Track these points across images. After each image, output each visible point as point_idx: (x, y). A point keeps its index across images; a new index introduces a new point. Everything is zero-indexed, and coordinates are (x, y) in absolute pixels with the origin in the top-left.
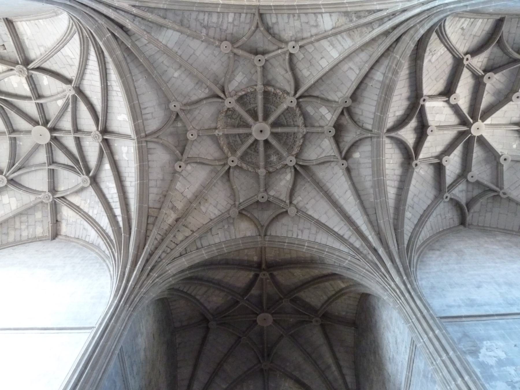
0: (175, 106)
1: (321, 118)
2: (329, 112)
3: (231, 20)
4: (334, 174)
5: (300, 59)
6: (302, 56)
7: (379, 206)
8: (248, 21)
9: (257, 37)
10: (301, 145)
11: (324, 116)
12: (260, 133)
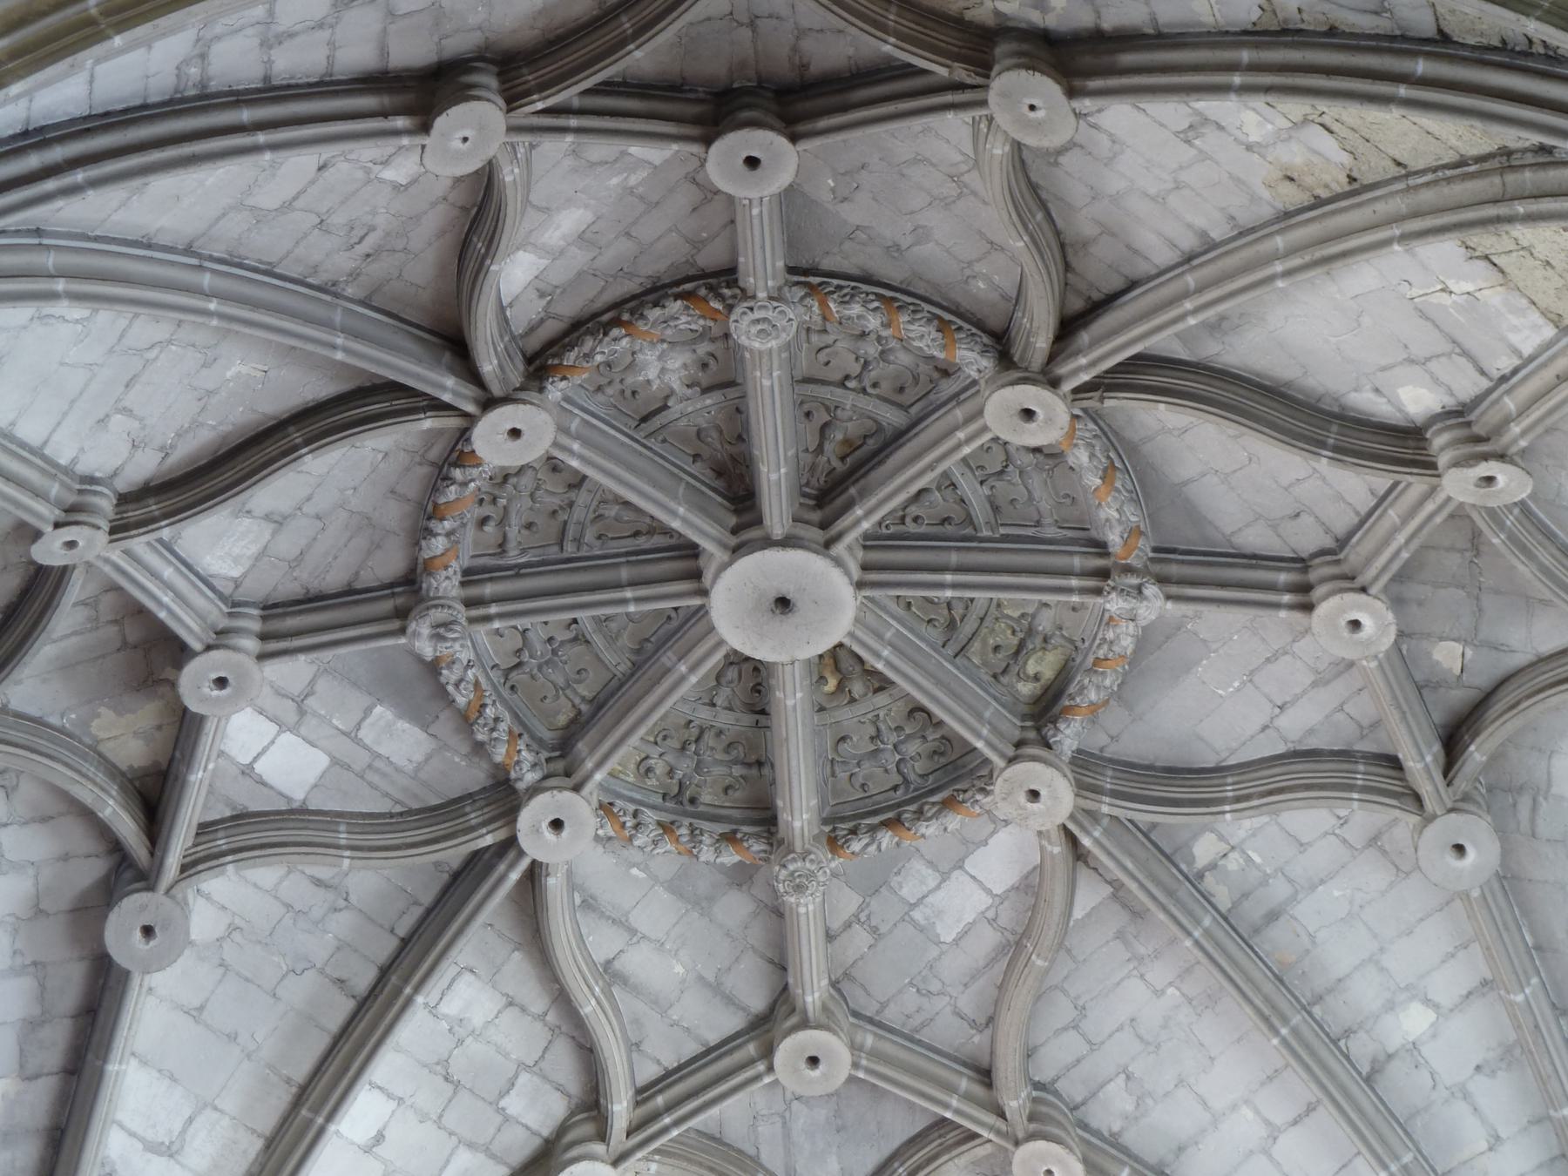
0: (1460, 849)
1: (300, 703)
2: (247, 771)
5: (524, 1078)
6: (514, 1104)
10: (436, 513)
11: (282, 726)
12: (790, 591)
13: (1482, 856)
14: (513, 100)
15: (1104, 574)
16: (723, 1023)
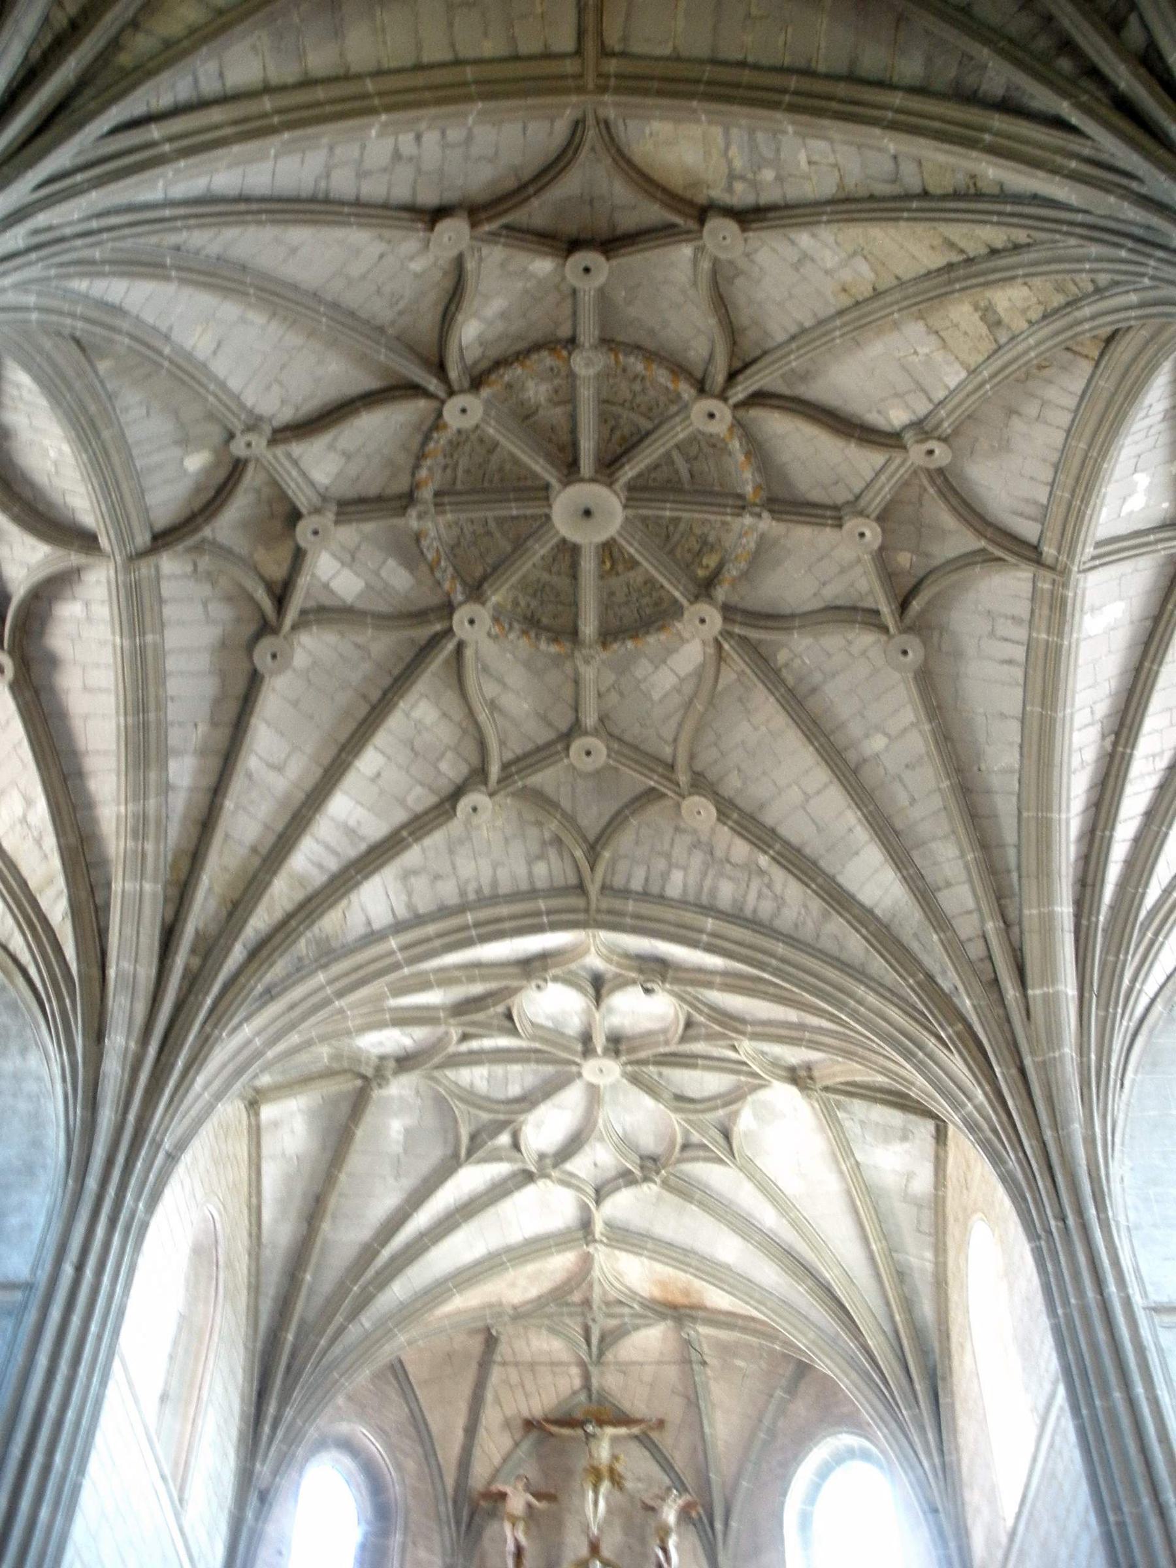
0: (905, 653)
2: (326, 586)
3: (677, 876)
4: (280, 383)
6: (444, 766)
7: (70, 373)
8: (623, 866)
9: (595, 810)
12: (593, 508)
13: (915, 655)
14: (474, 225)
15: (743, 508)
16: (544, 735)
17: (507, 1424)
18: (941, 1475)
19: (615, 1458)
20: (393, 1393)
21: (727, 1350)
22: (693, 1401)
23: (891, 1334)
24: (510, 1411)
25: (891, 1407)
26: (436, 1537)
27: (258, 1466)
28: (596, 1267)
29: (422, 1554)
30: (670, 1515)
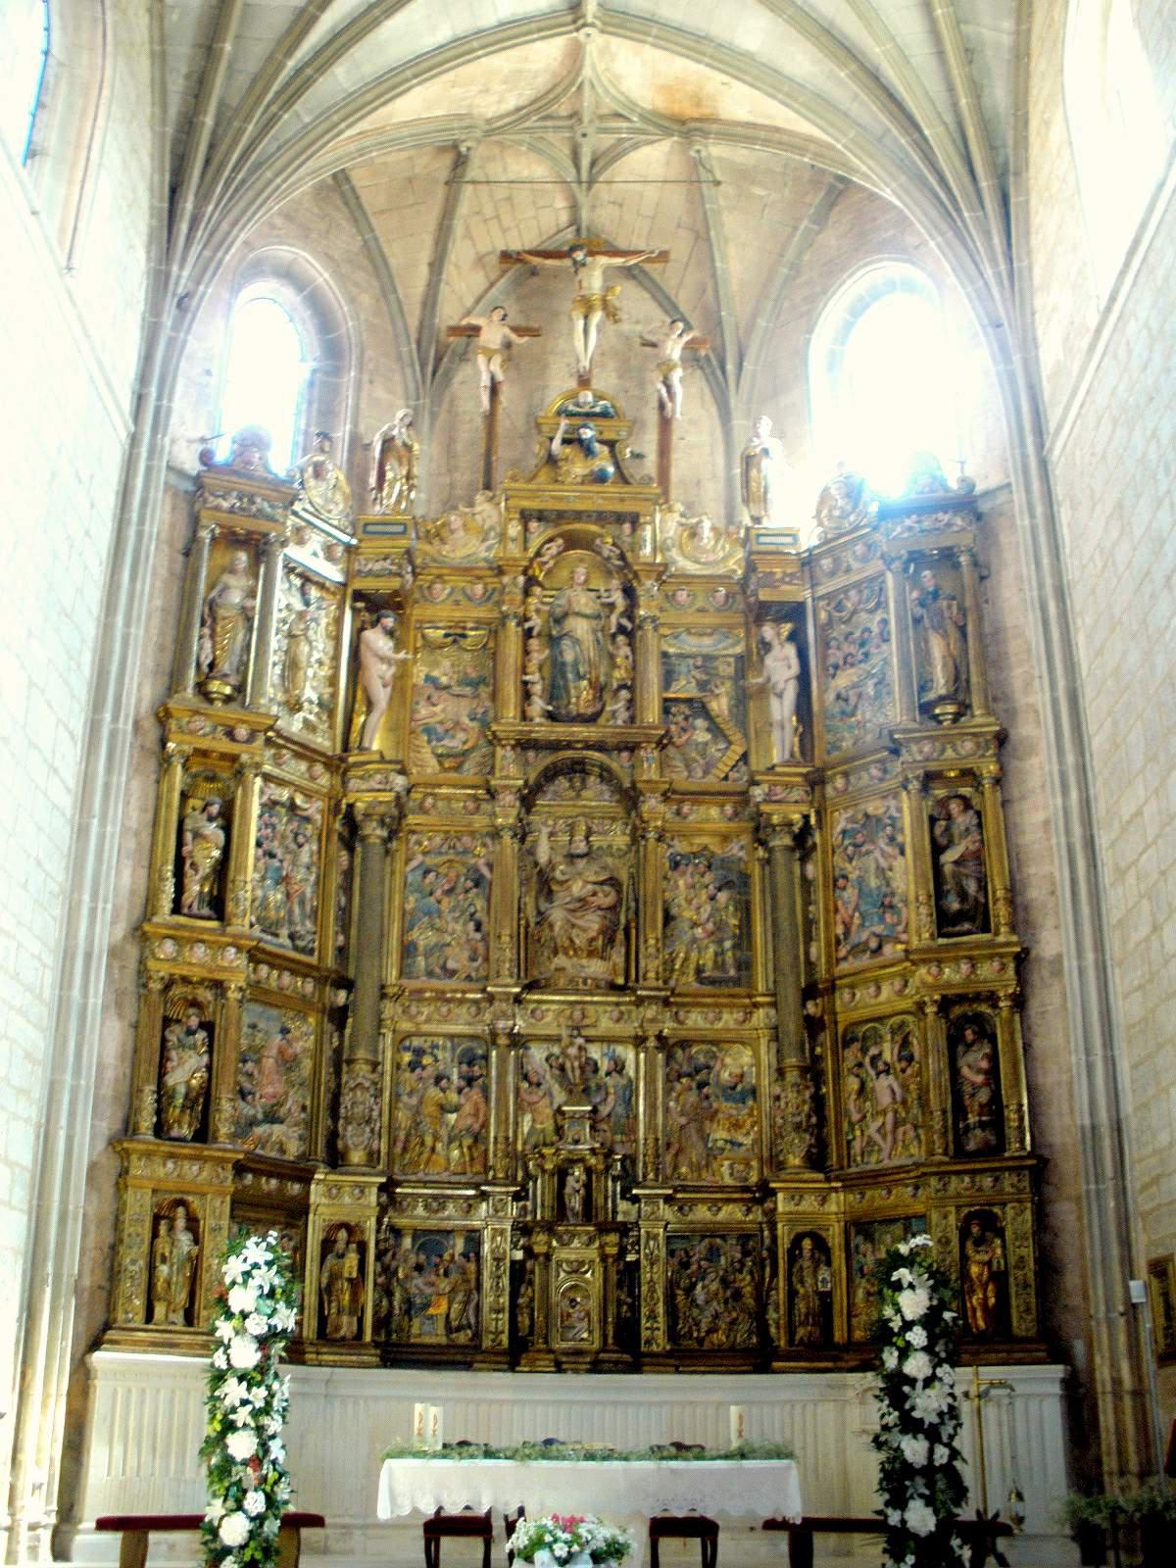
17: (480, 260)
18: (1006, 283)
19: (608, 289)
20: (341, 217)
21: (745, 176)
22: (703, 235)
23: (952, 126)
24: (483, 247)
25: (949, 211)
26: (397, 378)
27: (175, 269)
28: (587, 62)
29: (380, 393)
30: (674, 349)
